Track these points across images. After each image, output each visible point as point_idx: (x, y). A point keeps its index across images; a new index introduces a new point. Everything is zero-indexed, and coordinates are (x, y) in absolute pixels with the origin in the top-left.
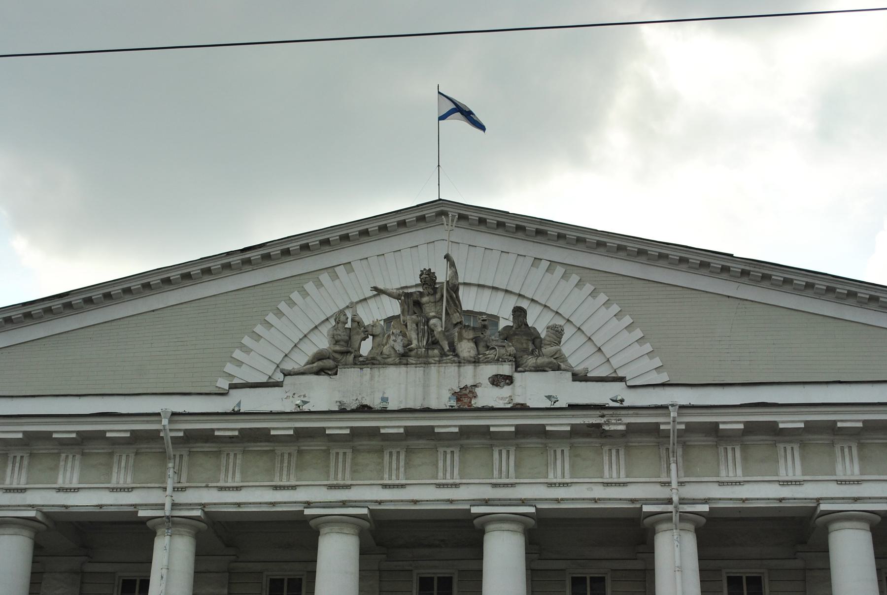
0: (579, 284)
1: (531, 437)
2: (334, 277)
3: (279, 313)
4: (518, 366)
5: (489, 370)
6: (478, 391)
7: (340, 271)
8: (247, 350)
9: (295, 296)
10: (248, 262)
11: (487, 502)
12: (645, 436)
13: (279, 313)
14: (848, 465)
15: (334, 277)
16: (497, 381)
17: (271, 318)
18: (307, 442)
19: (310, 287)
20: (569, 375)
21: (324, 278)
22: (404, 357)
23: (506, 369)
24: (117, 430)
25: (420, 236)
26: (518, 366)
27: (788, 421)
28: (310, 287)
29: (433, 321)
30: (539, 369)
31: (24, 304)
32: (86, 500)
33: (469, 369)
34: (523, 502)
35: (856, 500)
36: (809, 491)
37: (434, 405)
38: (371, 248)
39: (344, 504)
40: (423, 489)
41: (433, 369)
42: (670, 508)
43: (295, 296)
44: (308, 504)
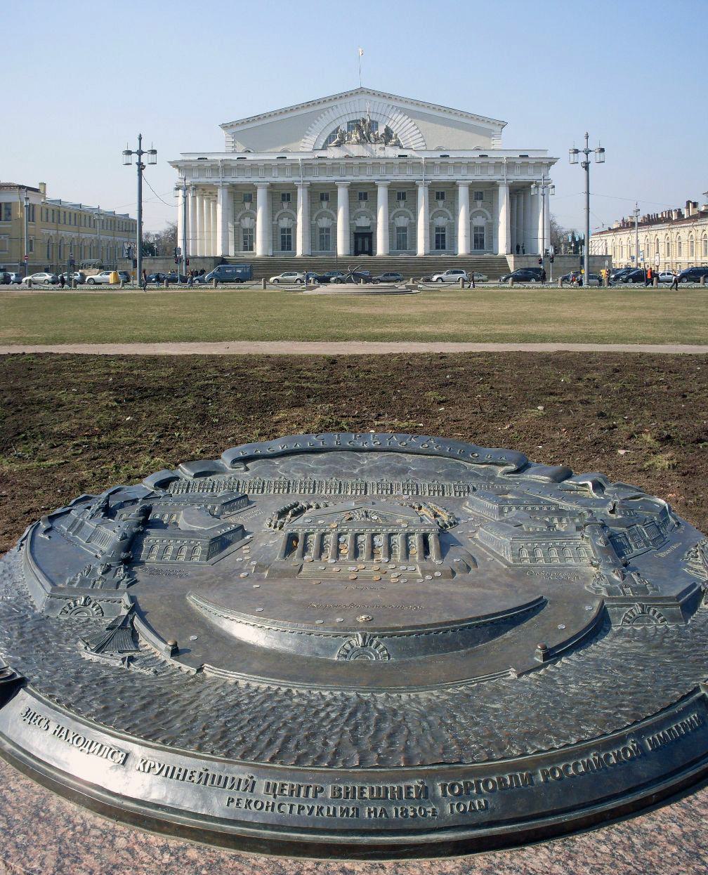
0: (400, 113)
1: (389, 164)
5: (380, 146)
9: (322, 115)
11: (379, 180)
12: (416, 165)
14: (464, 171)
16: (381, 149)
17: (316, 122)
18: (334, 166)
19: (326, 112)
21: (330, 110)
24: (288, 163)
25: (355, 98)
27: (451, 161)
28: (326, 112)
29: (365, 130)
30: (392, 146)
32: (281, 179)
34: (387, 180)
36: (455, 177)
38: (343, 101)
39: (344, 181)
40: (363, 178)
43: (322, 115)
44: (336, 181)
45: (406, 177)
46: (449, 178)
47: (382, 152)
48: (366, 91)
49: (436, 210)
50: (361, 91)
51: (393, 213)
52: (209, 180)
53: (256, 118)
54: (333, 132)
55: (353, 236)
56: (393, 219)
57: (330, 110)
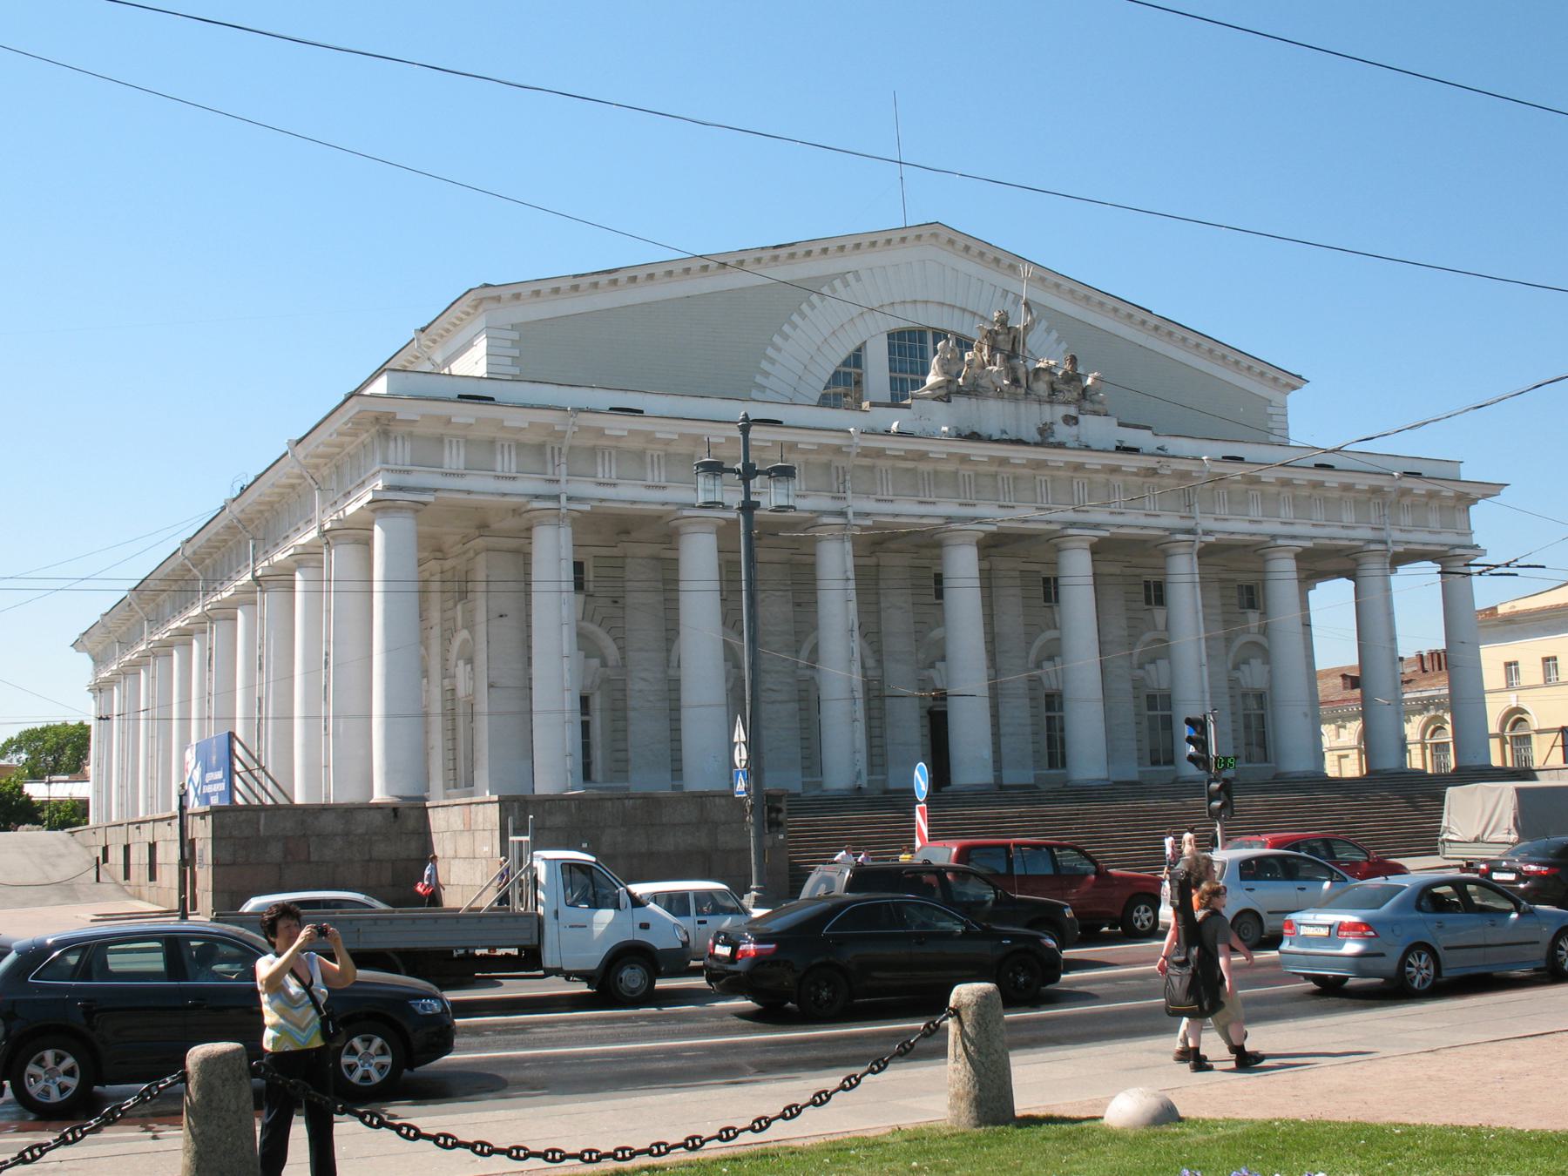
2: (846, 284)
3: (803, 316)
4: (1081, 411)
5: (1061, 411)
6: (1055, 427)
7: (850, 277)
8: (779, 350)
10: (776, 258)
13: (803, 316)
15: (846, 284)
16: (1070, 420)
20: (1115, 421)
21: (837, 283)
22: (1000, 394)
23: (1072, 411)
26: (1081, 411)
31: (575, 276)
33: (1047, 407)
34: (1096, 526)
35: (1294, 537)
37: (1025, 438)
41: (1022, 405)
42: (1191, 537)
45: (1143, 521)
46: (1254, 528)
47: (1074, 430)
48: (945, 235)
49: (1148, 636)
50: (935, 234)
51: (1038, 643)
52: (506, 486)
53: (604, 279)
54: (845, 363)
55: (926, 722)
56: (1039, 666)
57: (837, 283)
